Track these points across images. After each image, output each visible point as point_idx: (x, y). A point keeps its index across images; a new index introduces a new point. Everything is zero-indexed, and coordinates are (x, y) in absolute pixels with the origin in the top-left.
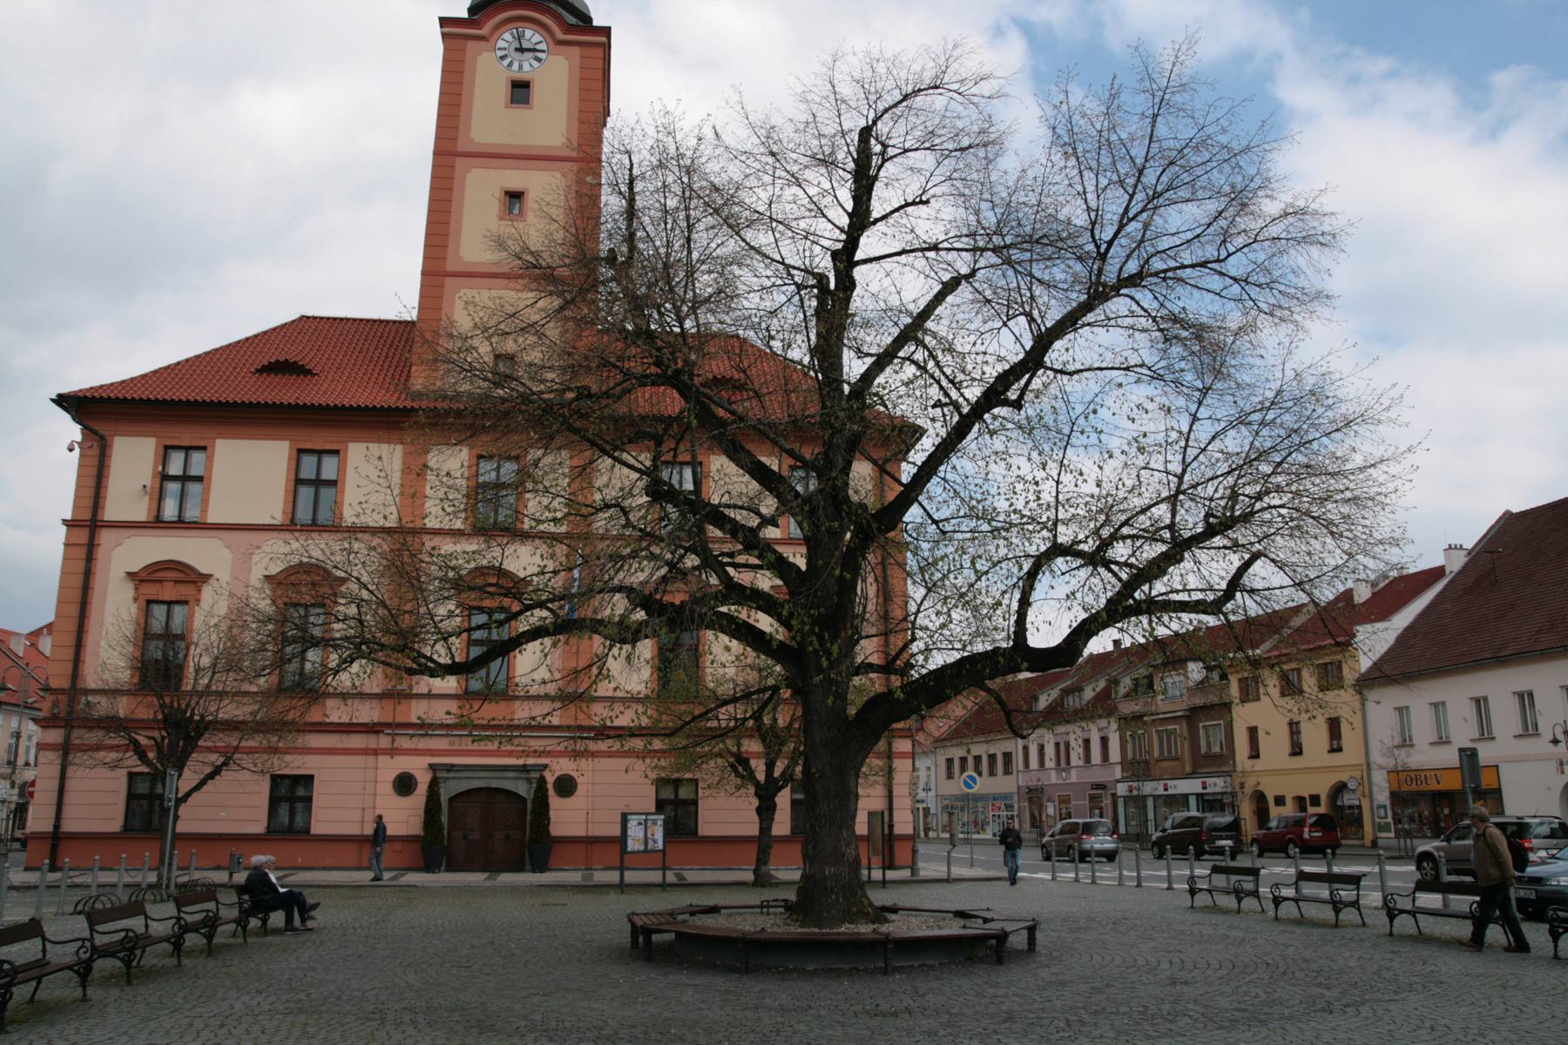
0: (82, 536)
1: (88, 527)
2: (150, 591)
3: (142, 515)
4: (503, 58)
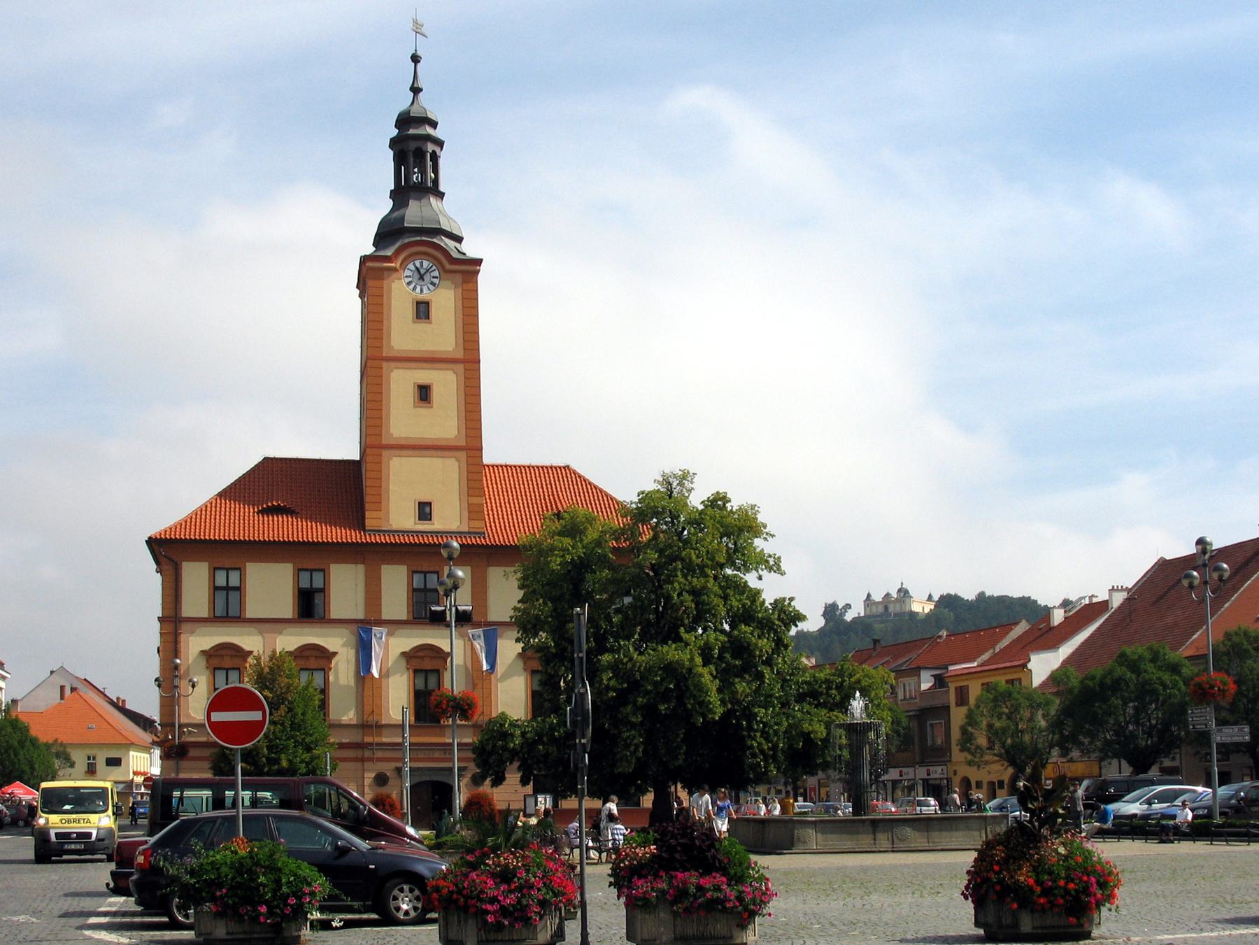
0: (170, 628)
1: (173, 622)
2: (216, 662)
3: (205, 614)
4: (409, 284)
